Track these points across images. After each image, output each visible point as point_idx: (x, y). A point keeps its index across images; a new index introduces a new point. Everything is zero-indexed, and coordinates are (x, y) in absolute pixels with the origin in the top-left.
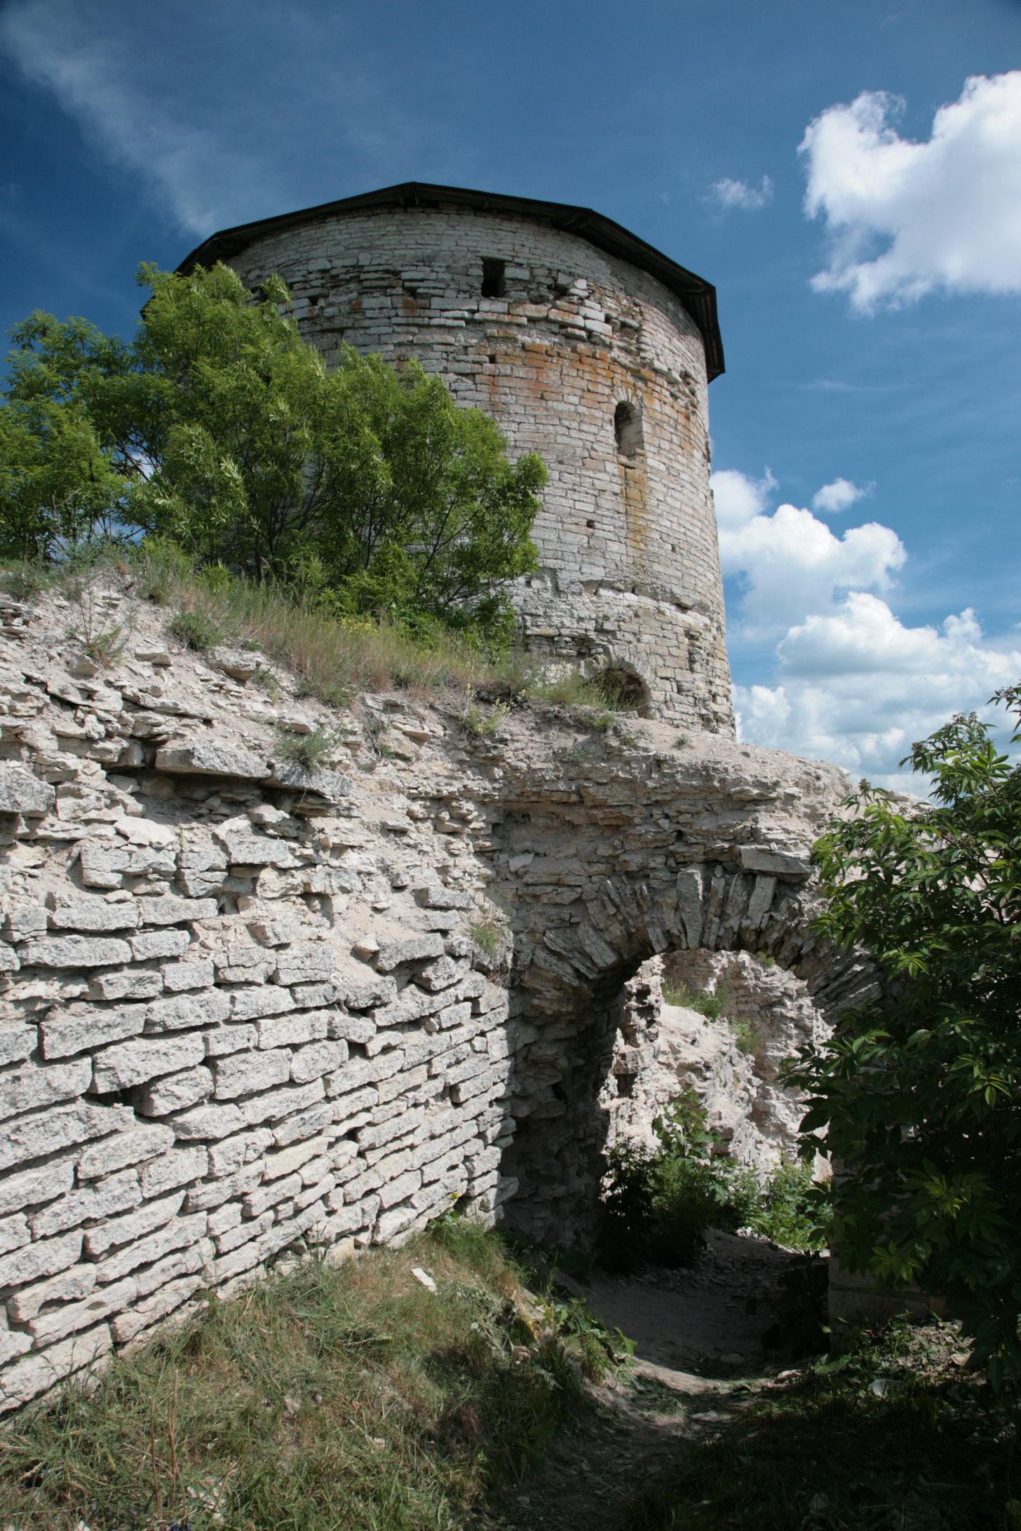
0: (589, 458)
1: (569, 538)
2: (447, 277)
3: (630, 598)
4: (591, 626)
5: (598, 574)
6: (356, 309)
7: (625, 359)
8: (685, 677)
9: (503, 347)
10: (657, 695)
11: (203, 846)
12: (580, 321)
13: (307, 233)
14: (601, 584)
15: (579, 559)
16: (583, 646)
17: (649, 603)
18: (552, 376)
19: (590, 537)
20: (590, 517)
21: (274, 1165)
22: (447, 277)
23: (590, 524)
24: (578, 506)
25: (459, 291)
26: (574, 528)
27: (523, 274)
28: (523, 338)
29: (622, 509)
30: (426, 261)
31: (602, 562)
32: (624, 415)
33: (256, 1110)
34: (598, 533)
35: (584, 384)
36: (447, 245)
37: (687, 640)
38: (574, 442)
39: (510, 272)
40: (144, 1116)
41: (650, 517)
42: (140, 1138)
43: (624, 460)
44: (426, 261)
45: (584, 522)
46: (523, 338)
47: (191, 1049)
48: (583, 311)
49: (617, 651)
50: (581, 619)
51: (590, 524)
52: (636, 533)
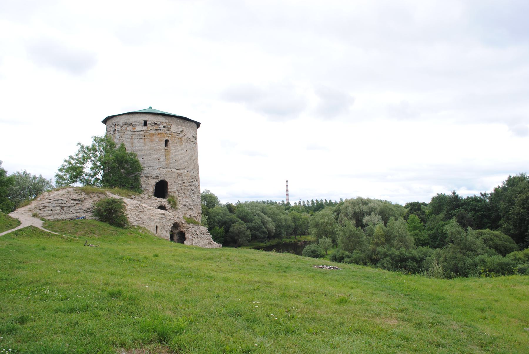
0: (160, 150)
3: (166, 169)
5: (160, 167)
7: (168, 132)
8: (176, 181)
9: (147, 134)
10: (169, 184)
11: (75, 202)
13: (120, 117)
16: (157, 177)
17: (170, 170)
18: (154, 138)
27: (150, 122)
28: (149, 132)
30: (136, 122)
32: (166, 142)
36: (139, 119)
43: (166, 148)
44: (136, 122)
46: (149, 132)
49: (161, 178)
52: (167, 160)
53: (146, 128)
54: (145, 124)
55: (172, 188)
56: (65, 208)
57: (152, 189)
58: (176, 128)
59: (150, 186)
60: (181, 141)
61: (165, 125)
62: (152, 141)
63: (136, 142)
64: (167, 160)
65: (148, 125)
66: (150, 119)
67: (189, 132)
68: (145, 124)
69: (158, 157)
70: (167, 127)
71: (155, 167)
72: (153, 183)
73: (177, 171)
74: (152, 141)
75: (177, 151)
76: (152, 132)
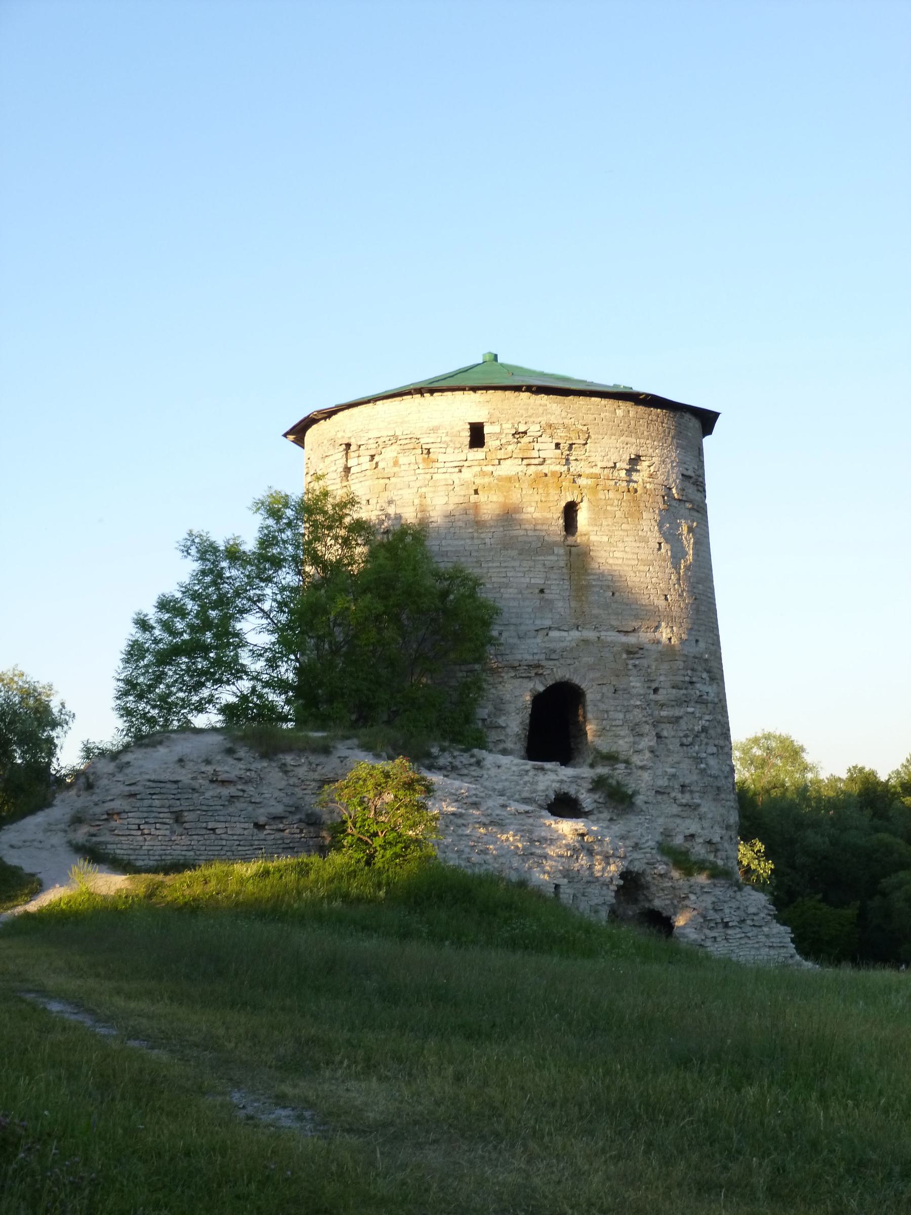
1: (527, 603)
2: (448, 439)
3: (575, 634)
4: (543, 657)
5: (548, 623)
6: (396, 463)
11: (225, 791)
12: (535, 454)
14: (550, 628)
15: (533, 616)
19: (542, 599)
20: (542, 587)
21: (240, 848)
22: (448, 439)
23: (542, 591)
24: (533, 581)
25: (455, 448)
26: (530, 596)
27: (496, 429)
29: (567, 577)
31: (550, 616)
33: (235, 837)
34: (546, 596)
35: (537, 498)
37: (625, 656)
38: (530, 539)
39: (486, 430)
40: (215, 833)
41: (591, 577)
42: (213, 837)
44: (435, 430)
45: (537, 591)
47: (223, 825)
48: (537, 446)
49: (560, 673)
50: (534, 654)
51: (542, 591)
53: (478, 454)
54: (477, 436)
56: (188, 816)
57: (515, 724)
59: (511, 708)
61: (561, 435)
65: (490, 442)
68: (477, 436)
69: (539, 581)
73: (624, 639)
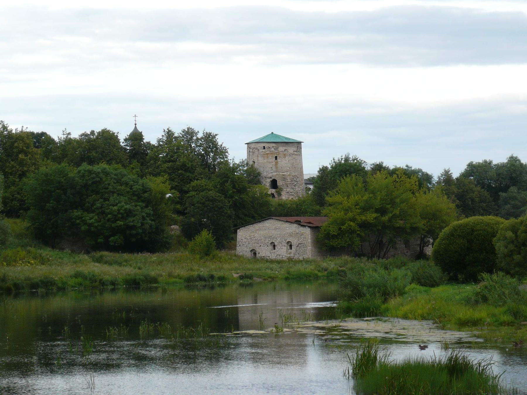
0: (272, 162)
49: (273, 178)
52: (277, 167)
54: (264, 148)
55: (280, 183)
58: (281, 149)
60: (285, 155)
62: (268, 157)
63: (260, 159)
64: (277, 167)
66: (266, 145)
67: (291, 150)
68: (264, 148)
70: (276, 149)
71: (270, 172)
72: (269, 180)
74: (268, 157)
75: (283, 162)
76: (268, 152)
